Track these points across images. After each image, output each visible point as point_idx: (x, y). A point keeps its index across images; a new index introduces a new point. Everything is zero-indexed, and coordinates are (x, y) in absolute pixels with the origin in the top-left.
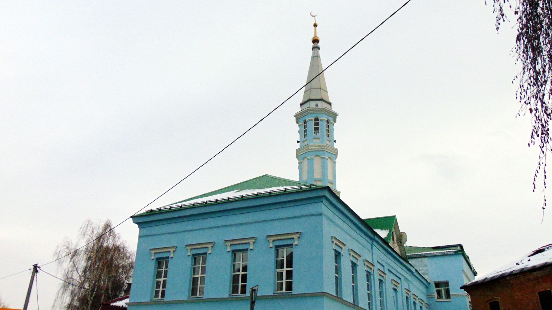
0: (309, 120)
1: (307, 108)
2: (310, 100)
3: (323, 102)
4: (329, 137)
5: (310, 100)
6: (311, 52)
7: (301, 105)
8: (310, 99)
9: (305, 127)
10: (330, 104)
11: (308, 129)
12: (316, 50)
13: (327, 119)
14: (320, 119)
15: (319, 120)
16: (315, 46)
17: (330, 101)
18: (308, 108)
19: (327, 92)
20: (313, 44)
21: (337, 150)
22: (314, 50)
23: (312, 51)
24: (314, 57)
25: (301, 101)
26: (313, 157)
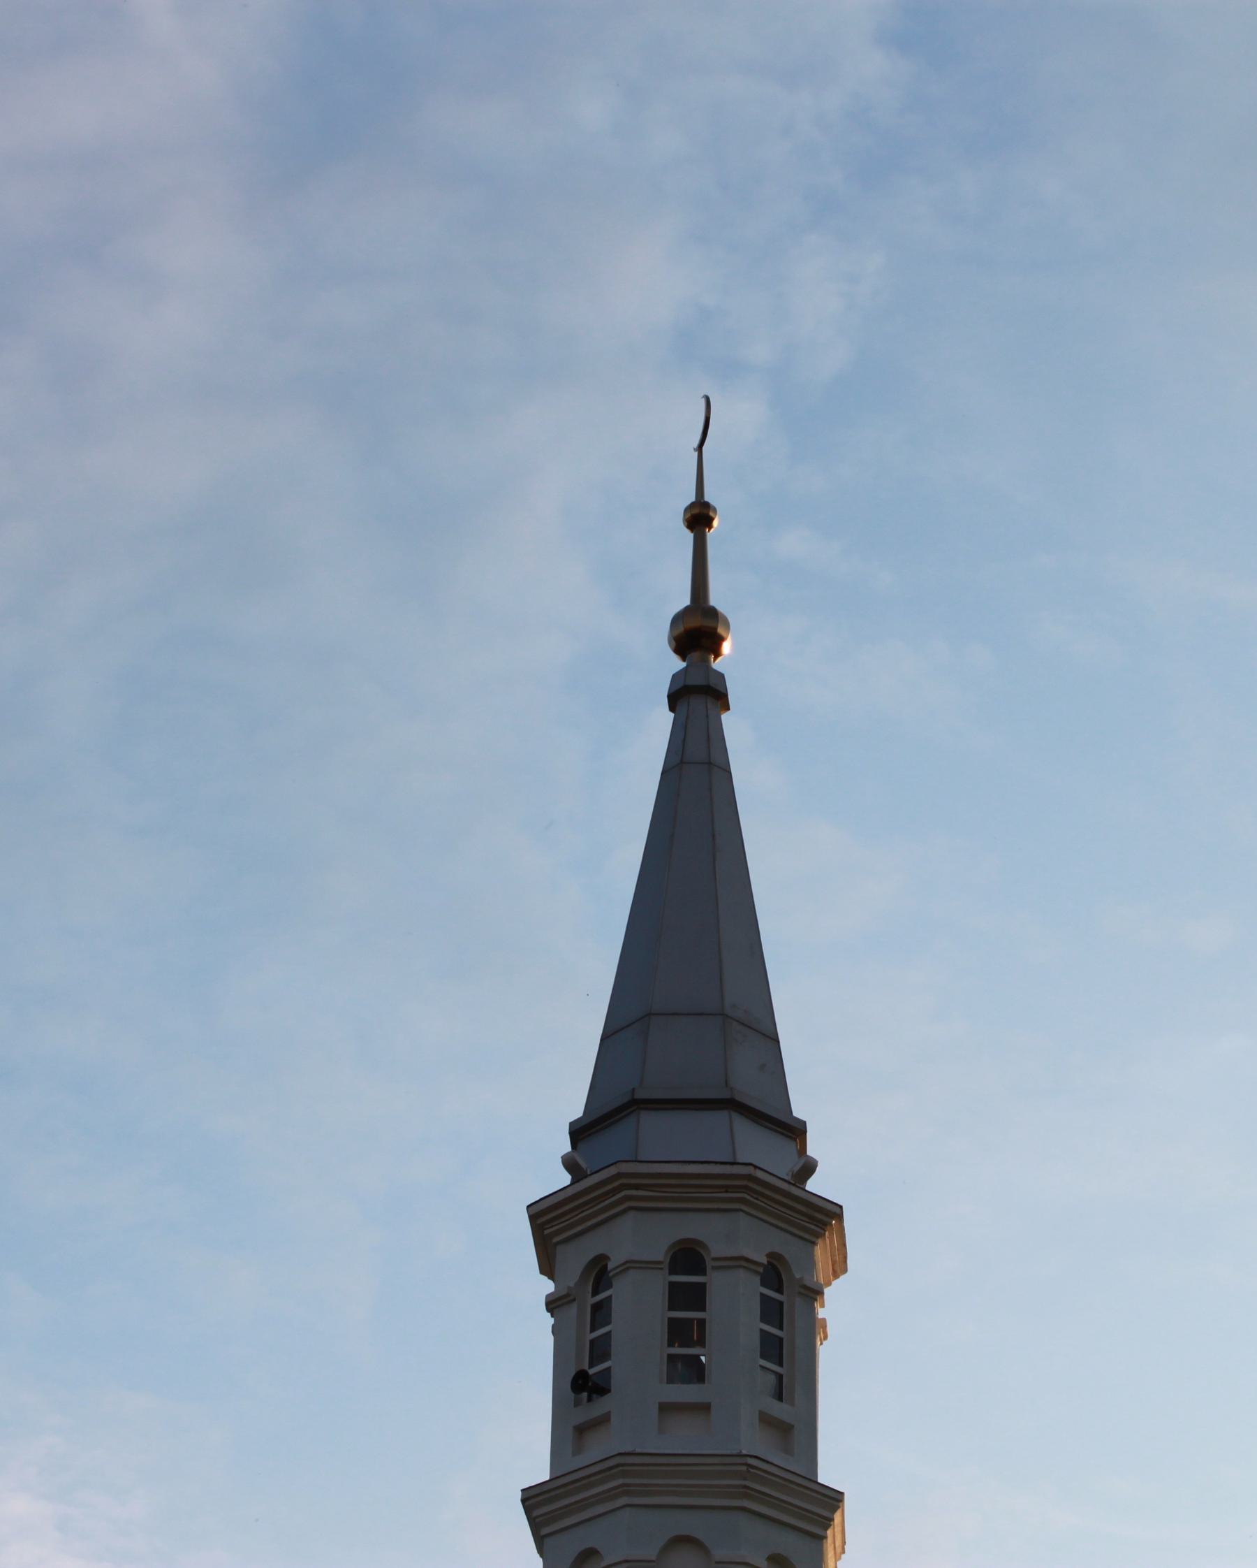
0: (628, 1266)
1: (612, 1171)
2: (635, 1105)
3: (736, 1116)
4: (780, 1397)
5: (635, 1105)
6: (662, 721)
7: (579, 1132)
8: (640, 1095)
9: (600, 1313)
10: (796, 1132)
11: (619, 1327)
12: (697, 703)
13: (771, 1255)
14: (717, 1249)
15: (709, 1264)
16: (696, 680)
17: (799, 1110)
18: (625, 1168)
19: (779, 1042)
20: (678, 664)
21: (834, 1499)
22: (678, 708)
23: (672, 715)
24: (682, 762)
25: (576, 1108)
26: (652, 1554)
